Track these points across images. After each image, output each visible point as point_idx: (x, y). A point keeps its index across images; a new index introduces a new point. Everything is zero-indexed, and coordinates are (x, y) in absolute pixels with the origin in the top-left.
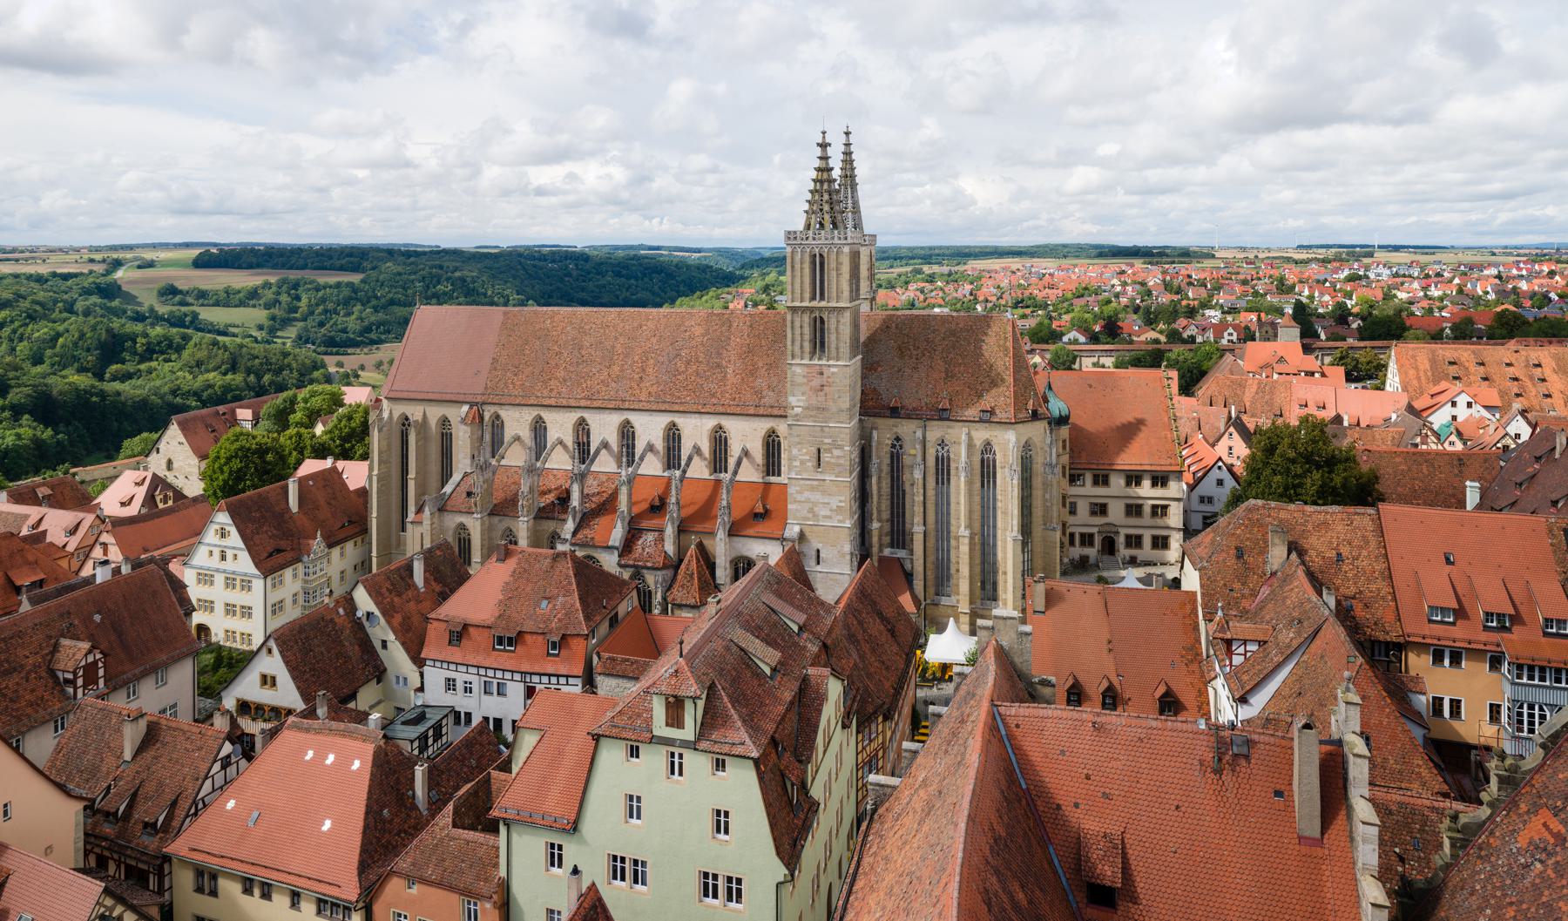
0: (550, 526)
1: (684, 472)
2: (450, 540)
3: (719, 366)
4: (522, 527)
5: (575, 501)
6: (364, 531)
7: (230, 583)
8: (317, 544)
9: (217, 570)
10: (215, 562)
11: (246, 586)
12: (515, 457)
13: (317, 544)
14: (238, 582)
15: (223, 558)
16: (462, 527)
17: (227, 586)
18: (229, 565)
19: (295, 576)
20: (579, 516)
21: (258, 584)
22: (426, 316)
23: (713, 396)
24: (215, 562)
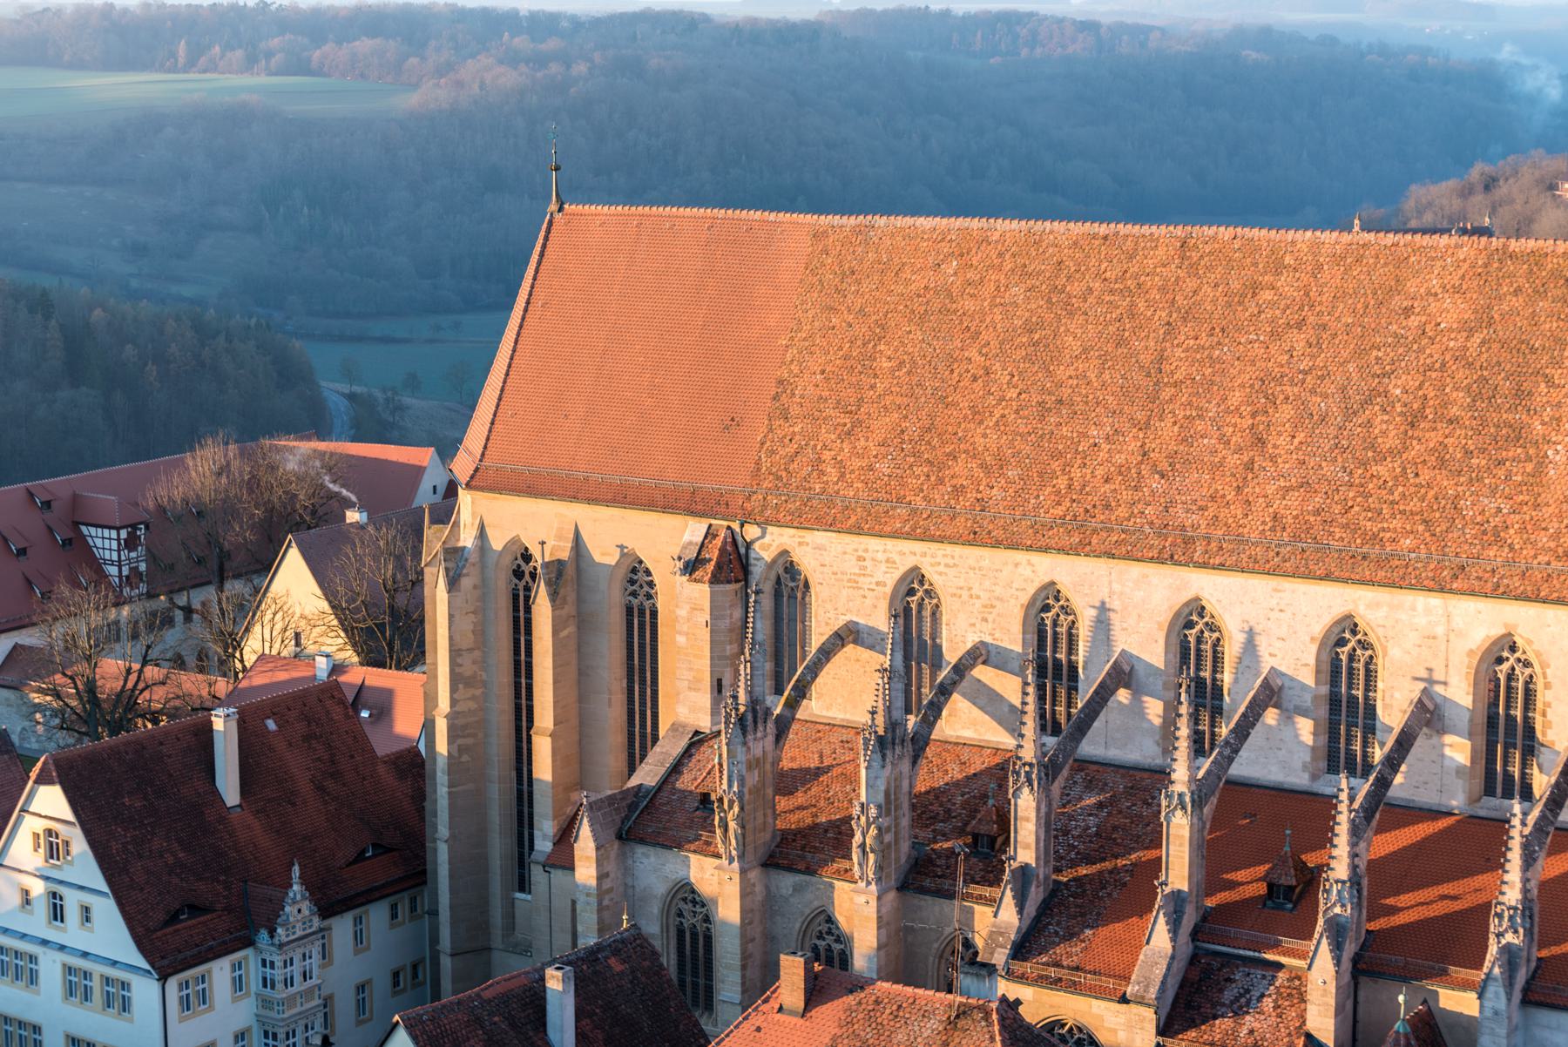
0: (940, 914)
1: (1383, 783)
2: (652, 928)
3: (1518, 435)
4: (858, 906)
5: (1026, 846)
6: (409, 872)
7: (76, 985)
8: (298, 907)
9: (45, 943)
10: (38, 923)
11: (118, 1000)
12: (847, 695)
13: (298, 907)
14: (96, 984)
15: (57, 913)
16: (687, 897)
17: (70, 990)
18: (72, 933)
19: (238, 984)
20: (1036, 895)
21: (145, 991)
22: (590, 240)
23: (1497, 538)
24: (38, 923)
